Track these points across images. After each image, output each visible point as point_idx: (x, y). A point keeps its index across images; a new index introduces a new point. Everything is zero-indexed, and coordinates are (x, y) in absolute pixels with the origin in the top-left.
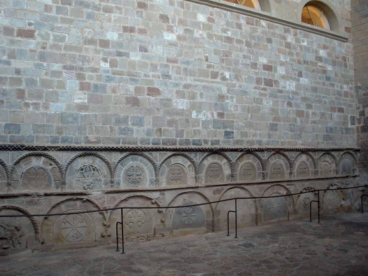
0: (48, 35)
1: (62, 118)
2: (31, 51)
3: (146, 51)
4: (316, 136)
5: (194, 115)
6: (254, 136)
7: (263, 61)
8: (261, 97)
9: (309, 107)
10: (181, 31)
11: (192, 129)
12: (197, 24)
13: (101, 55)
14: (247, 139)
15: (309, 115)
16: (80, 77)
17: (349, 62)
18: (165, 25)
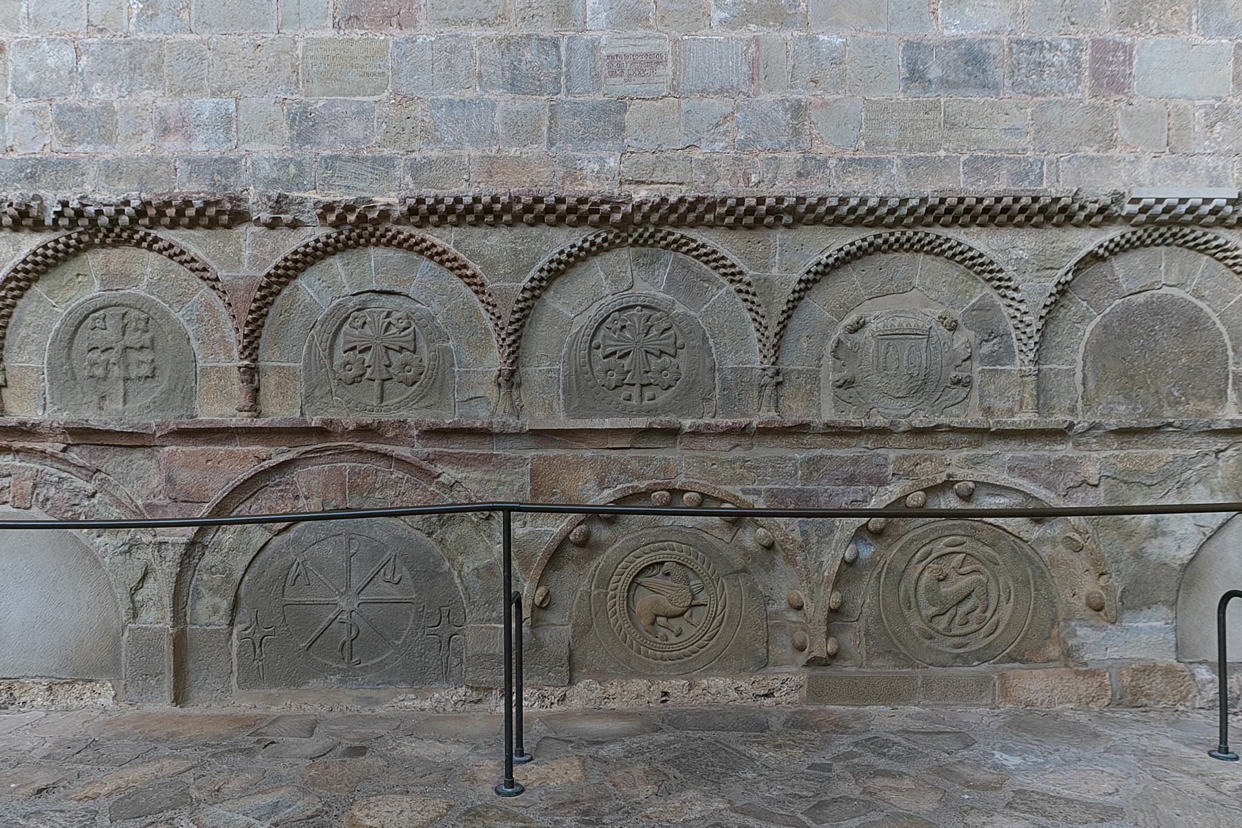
4: (783, 117)
6: (165, 131)
14: (107, 153)
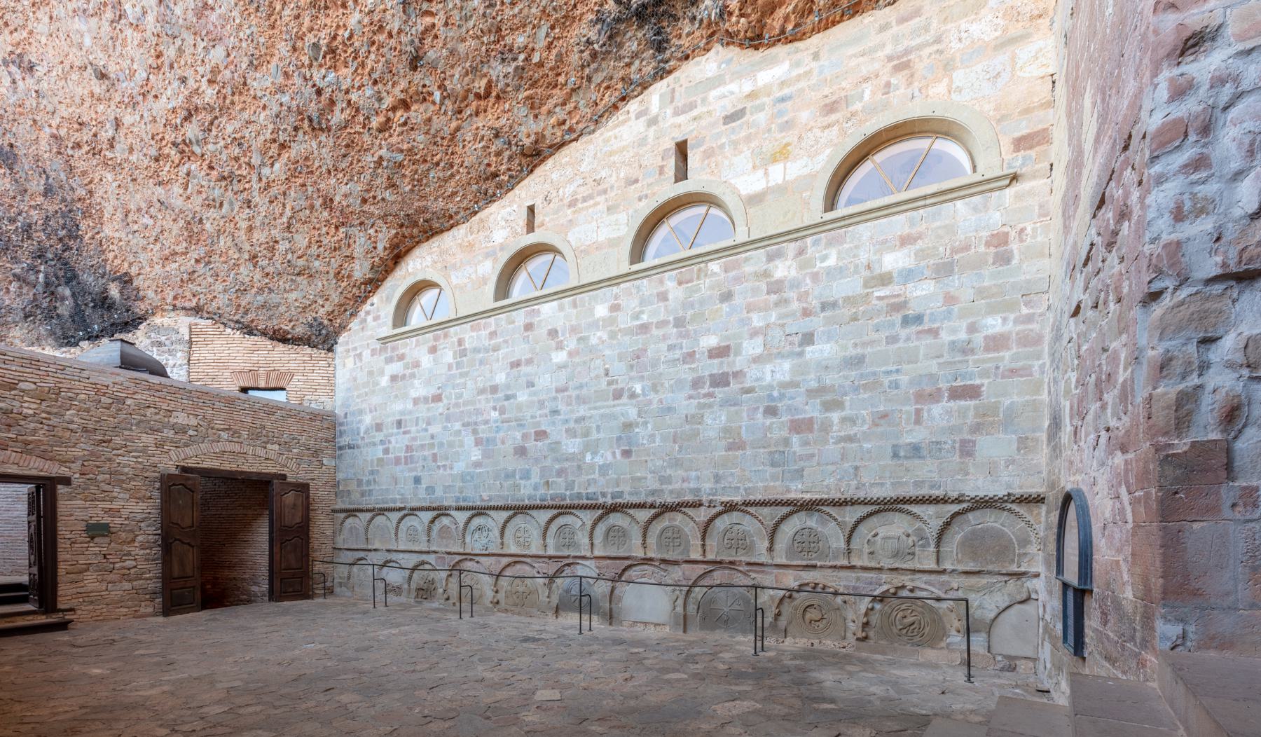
0: (451, 393)
1: (463, 477)
2: (441, 414)
3: (533, 386)
4: (852, 471)
5: (588, 457)
6: (684, 481)
7: (712, 341)
8: (702, 412)
9: (829, 406)
10: (572, 344)
11: (585, 478)
12: (595, 325)
13: (492, 404)
14: (670, 487)
15: (831, 426)
16: (475, 432)
17: (1021, 241)
18: (553, 343)
